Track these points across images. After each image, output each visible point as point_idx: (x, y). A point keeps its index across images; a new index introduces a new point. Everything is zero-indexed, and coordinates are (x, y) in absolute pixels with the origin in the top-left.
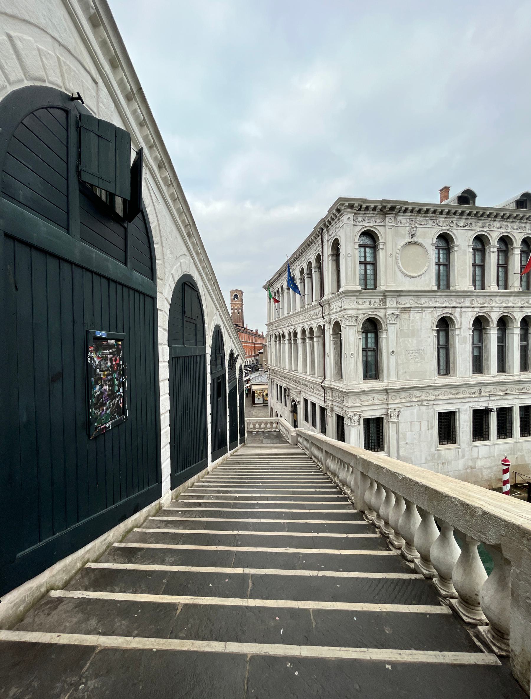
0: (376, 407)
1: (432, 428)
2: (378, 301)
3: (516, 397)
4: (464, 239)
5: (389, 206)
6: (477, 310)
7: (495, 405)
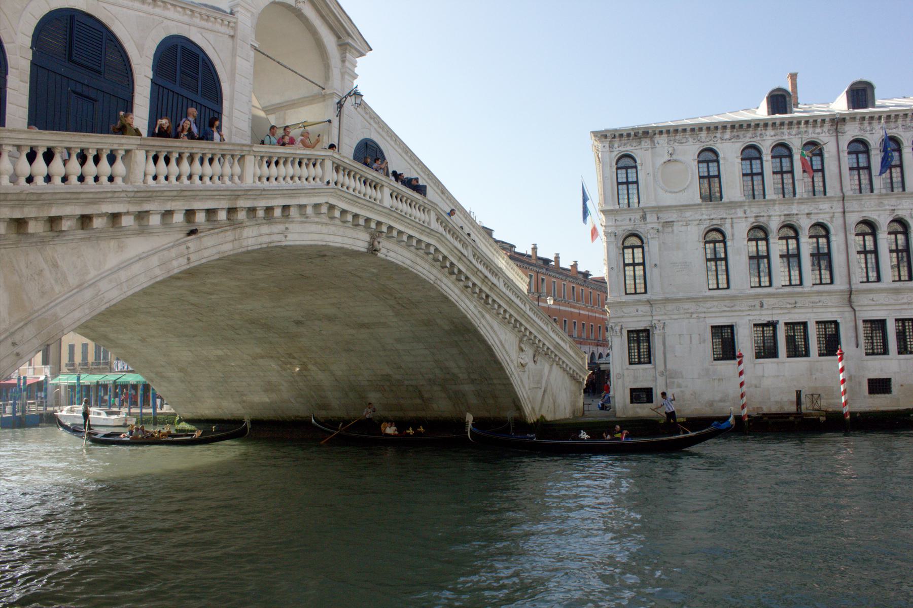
0: (639, 319)
1: (704, 341)
2: (638, 217)
3: (810, 310)
5: (641, 132)
6: (753, 220)
7: (782, 319)
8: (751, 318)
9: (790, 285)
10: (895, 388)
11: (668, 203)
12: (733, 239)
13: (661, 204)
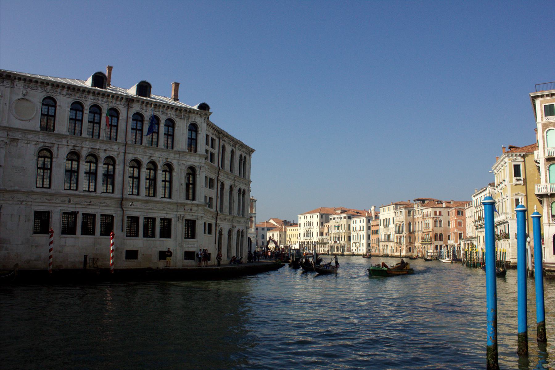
1: (29, 220)
3: (98, 207)
4: (64, 103)
6: (71, 147)
8: (61, 208)
9: (89, 191)
10: (140, 256)
11: (17, 126)
12: (57, 158)
13: (12, 126)
